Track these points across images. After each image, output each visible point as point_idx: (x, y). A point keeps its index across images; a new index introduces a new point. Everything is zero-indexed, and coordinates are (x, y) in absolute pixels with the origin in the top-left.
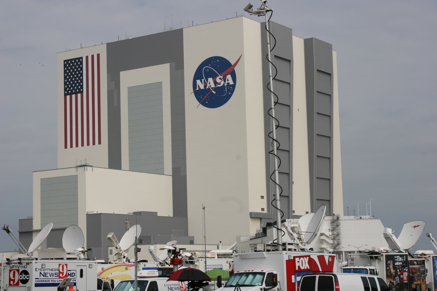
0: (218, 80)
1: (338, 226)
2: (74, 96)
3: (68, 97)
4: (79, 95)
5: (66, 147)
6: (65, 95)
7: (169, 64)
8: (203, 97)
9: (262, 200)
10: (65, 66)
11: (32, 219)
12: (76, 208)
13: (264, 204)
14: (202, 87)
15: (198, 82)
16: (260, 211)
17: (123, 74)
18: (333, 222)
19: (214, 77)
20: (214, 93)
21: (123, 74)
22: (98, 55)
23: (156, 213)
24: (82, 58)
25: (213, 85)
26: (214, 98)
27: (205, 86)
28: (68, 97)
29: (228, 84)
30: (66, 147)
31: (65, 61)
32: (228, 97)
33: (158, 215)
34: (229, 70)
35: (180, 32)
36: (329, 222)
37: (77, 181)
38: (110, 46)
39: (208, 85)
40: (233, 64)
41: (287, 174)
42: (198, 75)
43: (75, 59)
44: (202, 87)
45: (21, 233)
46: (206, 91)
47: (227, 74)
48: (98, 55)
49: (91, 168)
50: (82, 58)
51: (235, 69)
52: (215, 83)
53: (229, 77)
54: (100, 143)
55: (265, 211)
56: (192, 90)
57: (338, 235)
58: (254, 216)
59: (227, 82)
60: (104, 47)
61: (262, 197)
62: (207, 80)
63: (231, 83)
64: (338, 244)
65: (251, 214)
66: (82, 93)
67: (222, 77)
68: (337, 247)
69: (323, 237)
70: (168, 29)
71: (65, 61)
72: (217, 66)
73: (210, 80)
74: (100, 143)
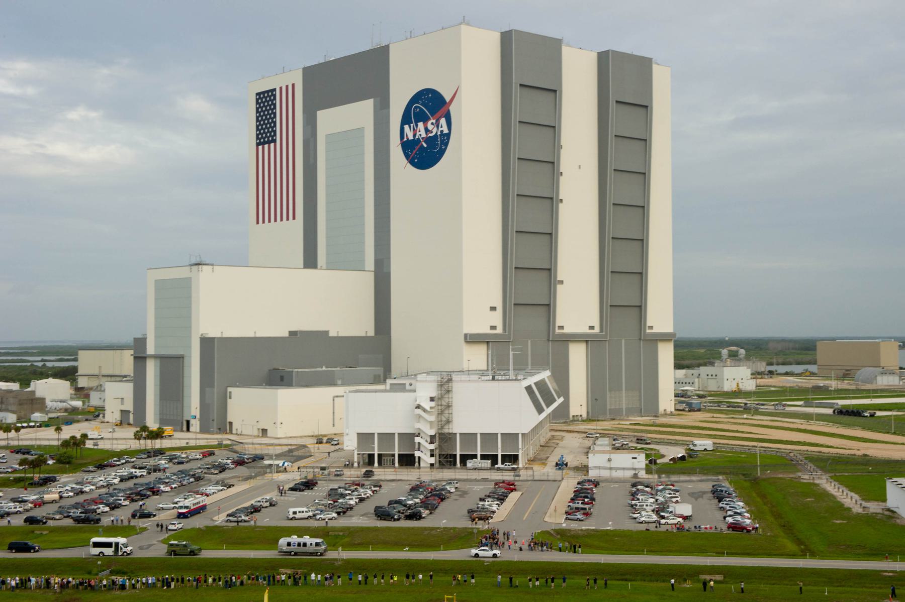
0: (430, 127)
1: (448, 391)
5: (258, 223)
6: (258, 145)
7: (371, 101)
8: (412, 152)
9: (493, 312)
11: (145, 339)
12: (189, 328)
13: (497, 319)
14: (411, 138)
15: (406, 127)
16: (488, 331)
18: (441, 386)
19: (425, 120)
20: (425, 145)
21: (319, 113)
22: (293, 85)
23: (327, 332)
24: (275, 90)
25: (424, 135)
27: (414, 135)
28: (260, 147)
29: (442, 131)
30: (258, 223)
31: (257, 94)
32: (442, 153)
33: (331, 334)
34: (443, 111)
35: (387, 47)
36: (435, 385)
37: (190, 287)
38: (305, 70)
39: (418, 134)
40: (448, 100)
41: (548, 272)
43: (268, 92)
44: (411, 138)
45: (135, 358)
46: (416, 142)
47: (441, 117)
48: (293, 85)
49: (210, 267)
50: (275, 90)
51: (451, 108)
52: (427, 130)
53: (443, 121)
54: (294, 218)
55: (499, 330)
56: (398, 141)
57: (449, 406)
58: (472, 339)
59: (440, 129)
60: (300, 73)
61: (493, 309)
62: (417, 126)
63: (446, 131)
64: (448, 422)
65: (466, 335)
66: (274, 141)
67: (434, 121)
68: (446, 427)
69: (419, 411)
70: (375, 46)
72: (430, 104)
73: (421, 125)
74: (294, 218)
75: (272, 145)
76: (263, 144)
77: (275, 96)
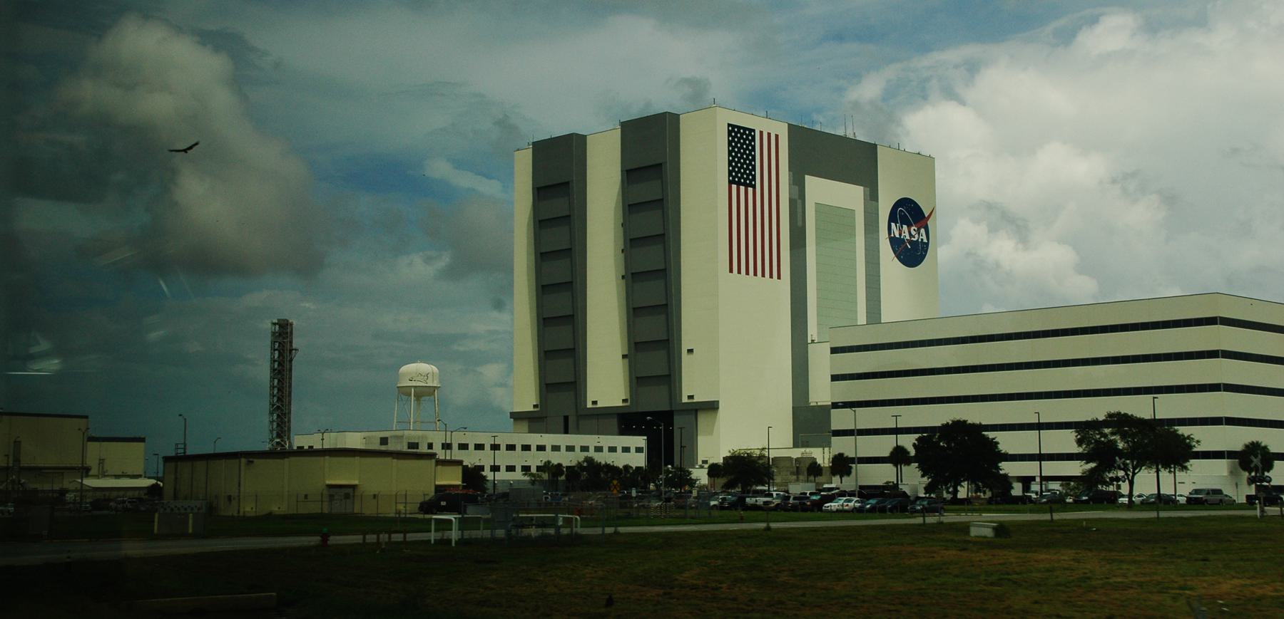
2: (742, 188)
3: (734, 187)
4: (750, 189)
5: (731, 271)
10: (730, 133)
17: (810, 180)
19: (909, 226)
22: (777, 136)
26: (912, 254)
28: (734, 187)
30: (731, 271)
31: (729, 125)
32: (923, 257)
38: (793, 129)
42: (892, 218)
48: (777, 136)
51: (929, 223)
53: (923, 231)
54: (779, 277)
66: (754, 187)
71: (729, 125)
73: (905, 227)
74: (779, 277)
75: (750, 189)
76: (739, 184)
77: (754, 137)
